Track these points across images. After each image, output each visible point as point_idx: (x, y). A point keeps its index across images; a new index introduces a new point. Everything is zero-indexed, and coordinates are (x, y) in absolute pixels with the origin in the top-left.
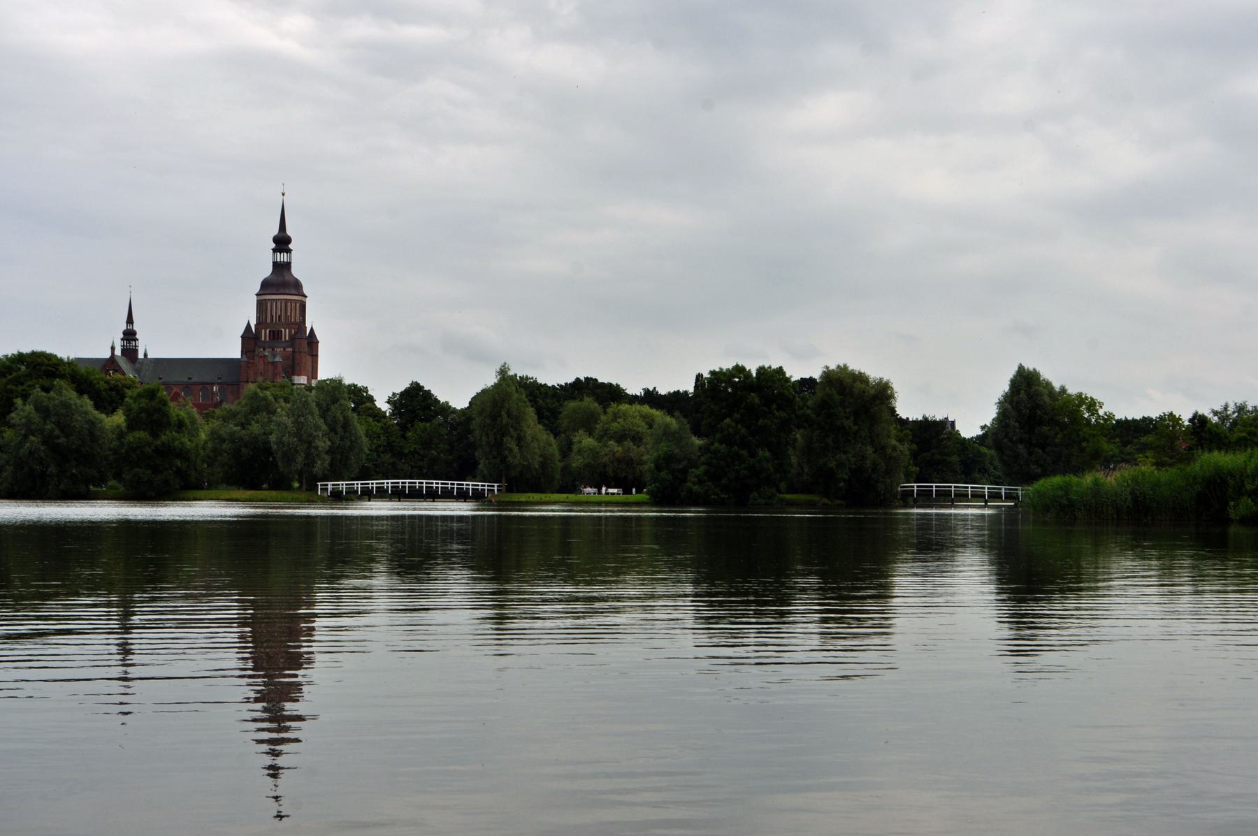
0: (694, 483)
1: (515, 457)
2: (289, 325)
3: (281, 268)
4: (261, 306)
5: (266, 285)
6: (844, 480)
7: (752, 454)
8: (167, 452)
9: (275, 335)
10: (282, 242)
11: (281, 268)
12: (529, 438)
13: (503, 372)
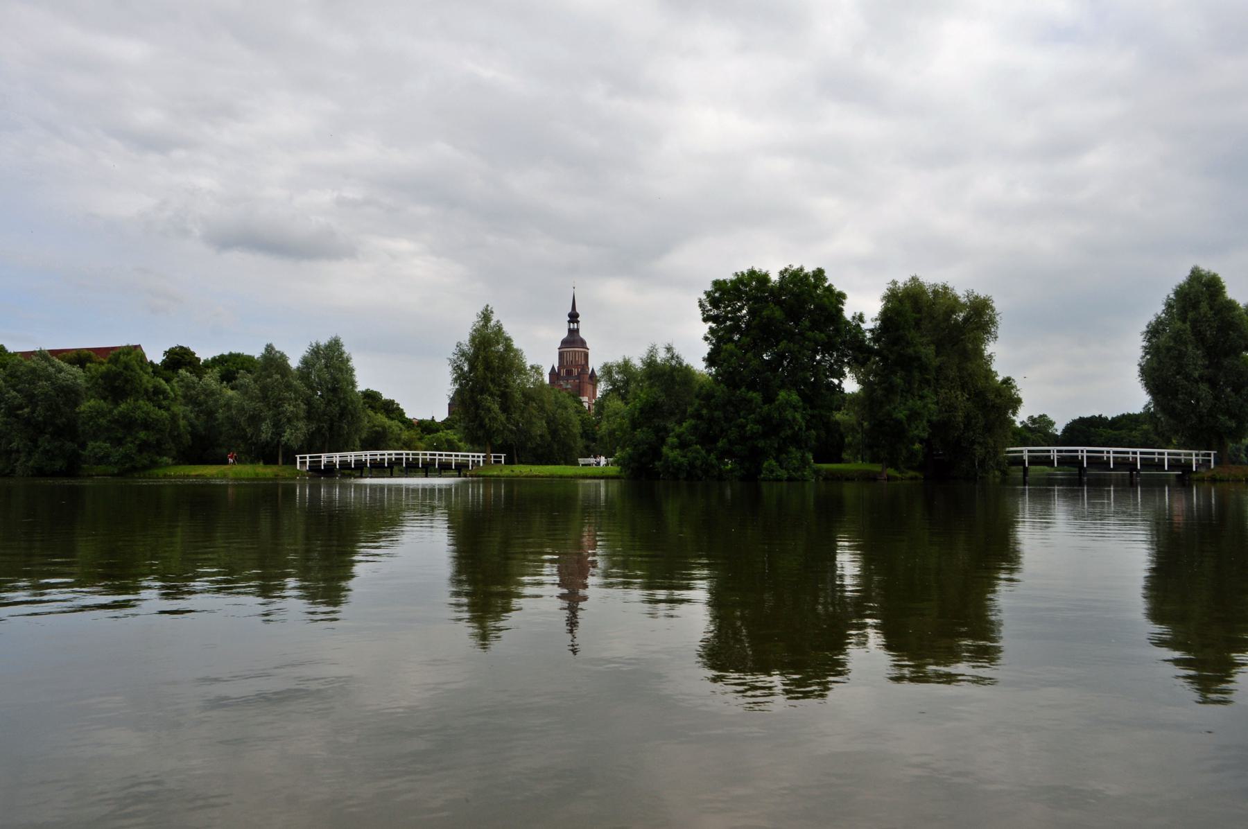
0: (673, 448)
1: (495, 419)
2: (577, 366)
3: (573, 333)
4: (561, 355)
5: (565, 343)
6: (921, 441)
7: (769, 399)
8: (128, 424)
9: (569, 373)
10: (574, 317)
11: (573, 333)
12: (518, 396)
13: (486, 316)
